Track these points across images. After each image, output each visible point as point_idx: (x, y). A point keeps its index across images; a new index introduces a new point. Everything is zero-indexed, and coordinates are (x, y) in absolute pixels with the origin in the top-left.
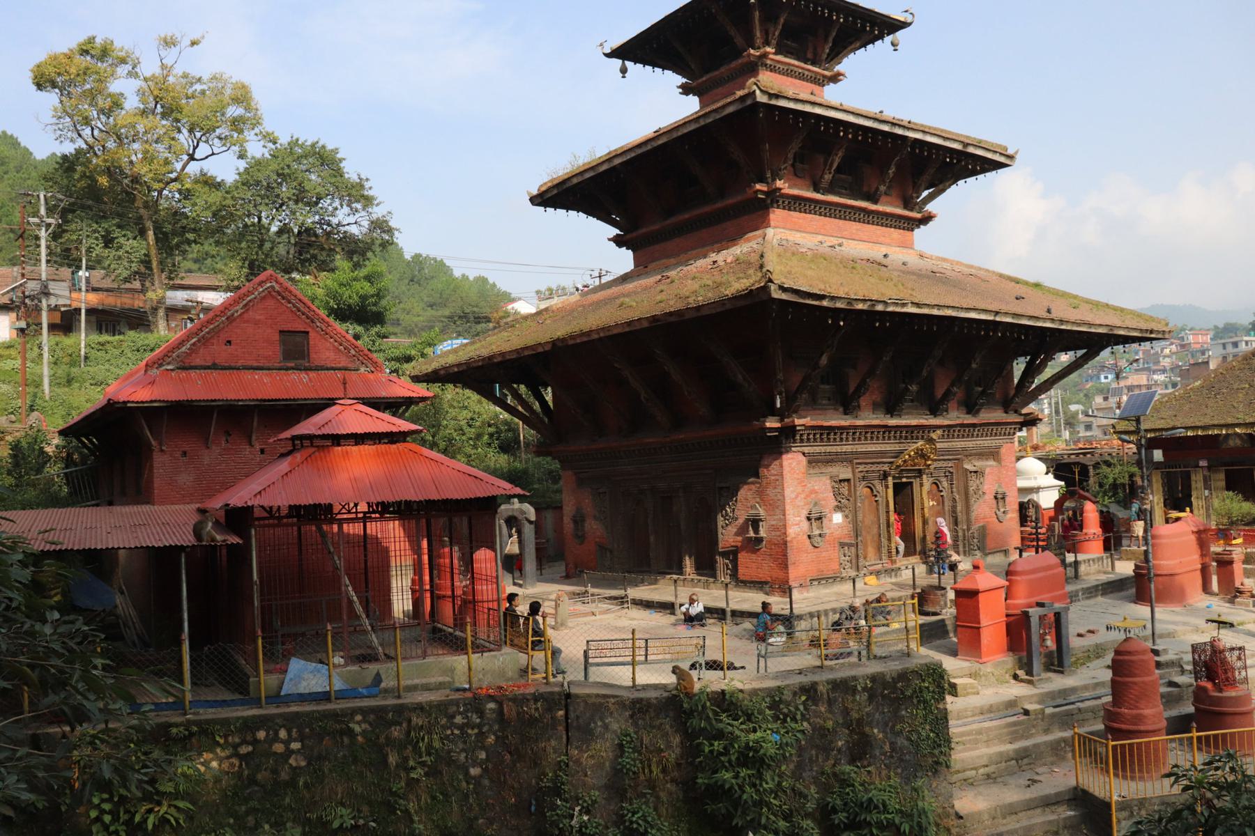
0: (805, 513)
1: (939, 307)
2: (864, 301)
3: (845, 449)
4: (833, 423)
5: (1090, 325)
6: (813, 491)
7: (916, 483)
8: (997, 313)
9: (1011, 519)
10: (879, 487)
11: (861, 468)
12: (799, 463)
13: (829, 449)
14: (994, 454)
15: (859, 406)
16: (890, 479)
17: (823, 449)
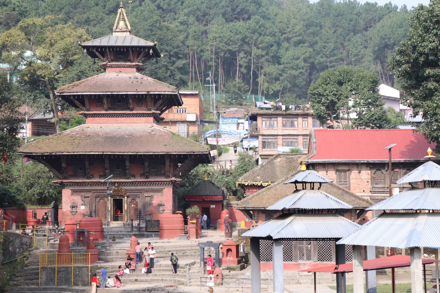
0: (69, 205)
1: (77, 152)
2: (47, 153)
3: (87, 188)
4: (81, 181)
5: (154, 153)
6: (73, 200)
8: (103, 152)
9: (167, 213)
10: (106, 199)
11: (96, 194)
12: (68, 192)
13: (80, 188)
14: (160, 191)
15: (93, 175)
17: (78, 188)
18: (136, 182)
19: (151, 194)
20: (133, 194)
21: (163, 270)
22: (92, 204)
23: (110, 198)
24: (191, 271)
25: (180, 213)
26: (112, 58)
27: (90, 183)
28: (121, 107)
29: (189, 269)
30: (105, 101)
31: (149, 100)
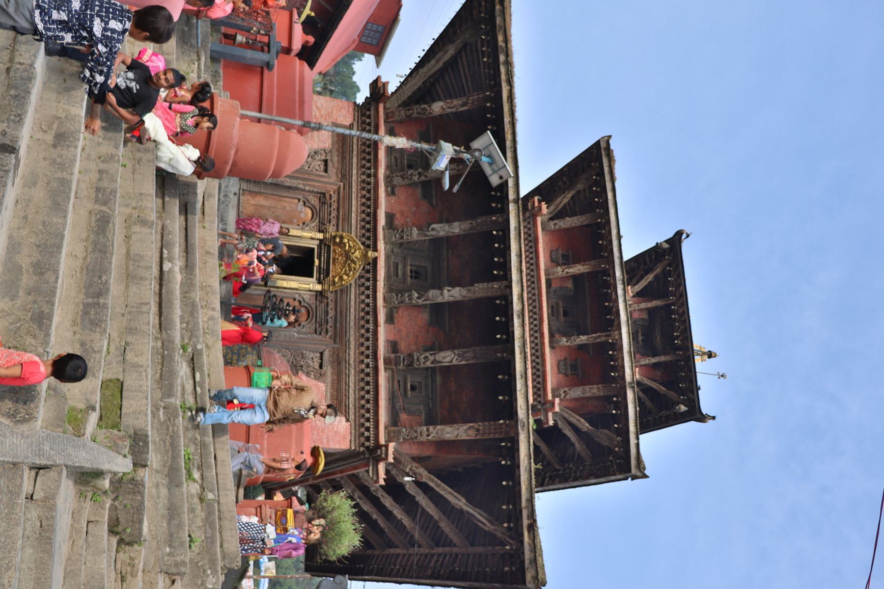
7: (314, 280)
11: (335, 198)
15: (393, 193)
16: (320, 236)
17: (355, 147)
18: (376, 324)
19: (328, 370)
20: (331, 314)
21: (102, 224)
22: (303, 179)
23: (320, 236)
24: (67, 489)
25: (316, 464)
26: (636, 315)
27: (372, 180)
28: (553, 315)
29: (85, 477)
30: (578, 269)
31: (593, 390)
